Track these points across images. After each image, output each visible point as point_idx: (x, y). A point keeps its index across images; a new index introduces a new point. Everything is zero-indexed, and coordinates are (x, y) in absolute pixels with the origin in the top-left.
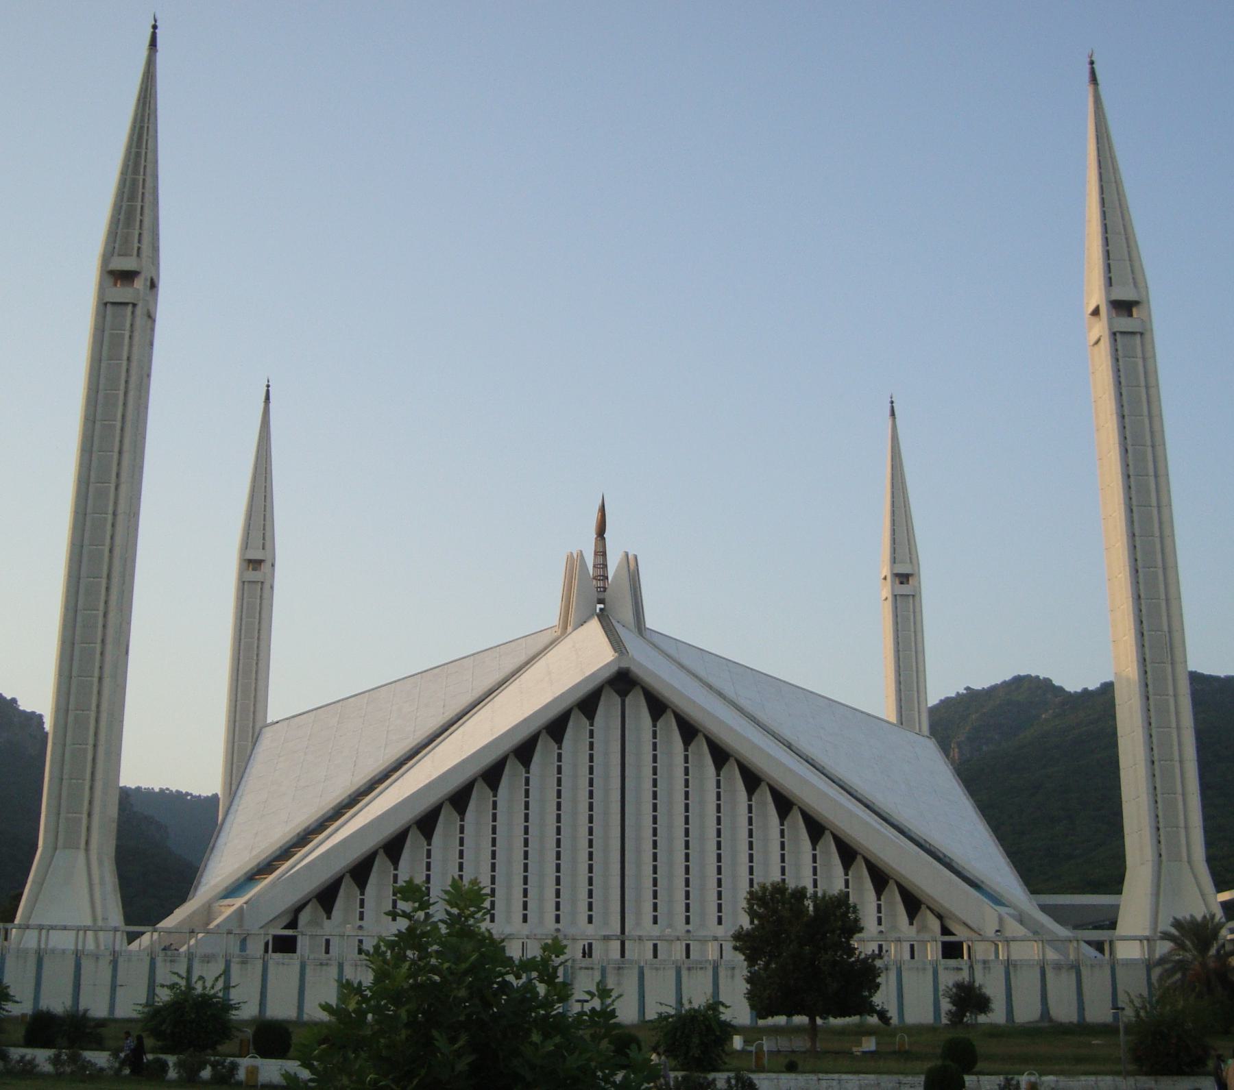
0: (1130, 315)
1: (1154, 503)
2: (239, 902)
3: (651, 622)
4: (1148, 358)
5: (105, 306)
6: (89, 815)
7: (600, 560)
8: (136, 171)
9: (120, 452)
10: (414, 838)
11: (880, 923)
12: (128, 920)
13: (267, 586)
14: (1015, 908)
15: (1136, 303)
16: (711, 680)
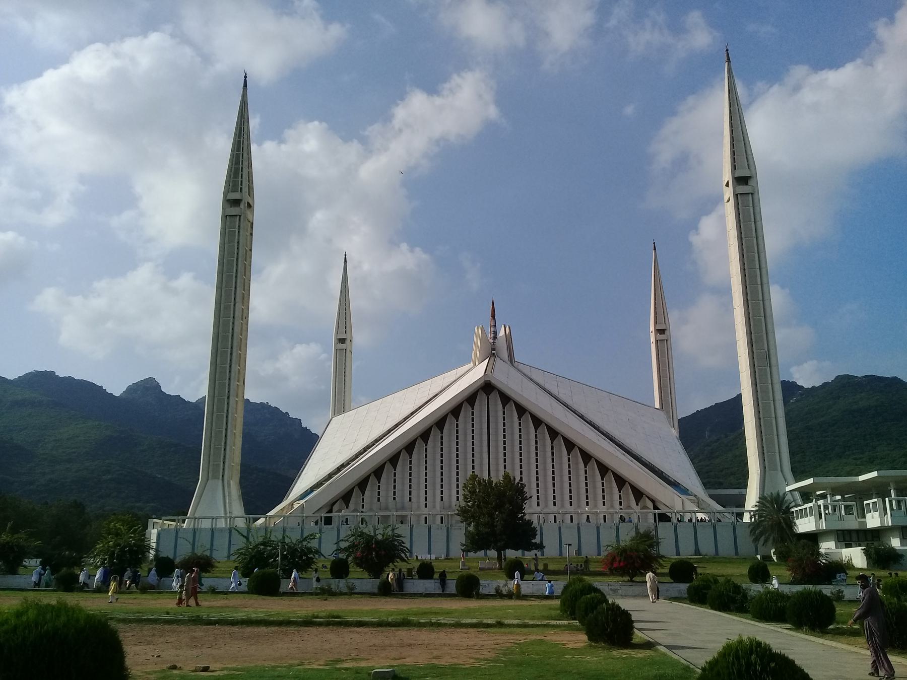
0: (747, 184)
1: (759, 282)
2: (302, 502)
3: (517, 358)
4: (755, 205)
5: (225, 217)
6: (224, 463)
7: (493, 329)
8: (238, 150)
9: (236, 288)
10: (388, 466)
11: (620, 503)
12: (248, 511)
13: (348, 351)
14: (695, 496)
15: (750, 177)
16: (547, 386)
